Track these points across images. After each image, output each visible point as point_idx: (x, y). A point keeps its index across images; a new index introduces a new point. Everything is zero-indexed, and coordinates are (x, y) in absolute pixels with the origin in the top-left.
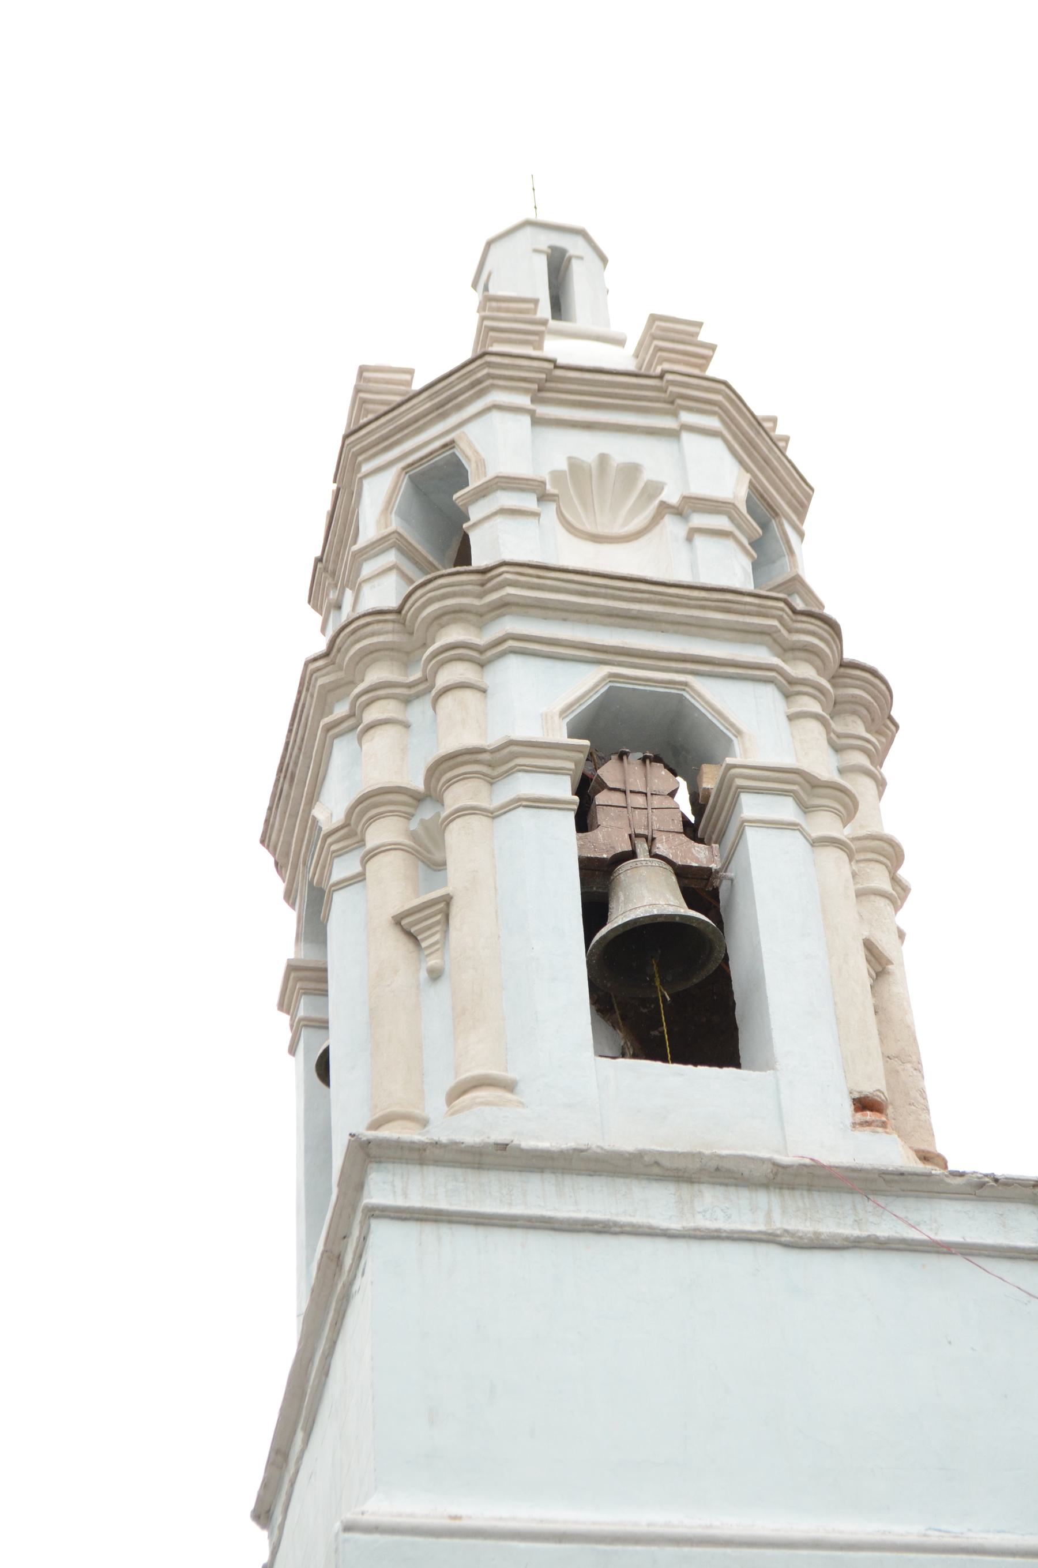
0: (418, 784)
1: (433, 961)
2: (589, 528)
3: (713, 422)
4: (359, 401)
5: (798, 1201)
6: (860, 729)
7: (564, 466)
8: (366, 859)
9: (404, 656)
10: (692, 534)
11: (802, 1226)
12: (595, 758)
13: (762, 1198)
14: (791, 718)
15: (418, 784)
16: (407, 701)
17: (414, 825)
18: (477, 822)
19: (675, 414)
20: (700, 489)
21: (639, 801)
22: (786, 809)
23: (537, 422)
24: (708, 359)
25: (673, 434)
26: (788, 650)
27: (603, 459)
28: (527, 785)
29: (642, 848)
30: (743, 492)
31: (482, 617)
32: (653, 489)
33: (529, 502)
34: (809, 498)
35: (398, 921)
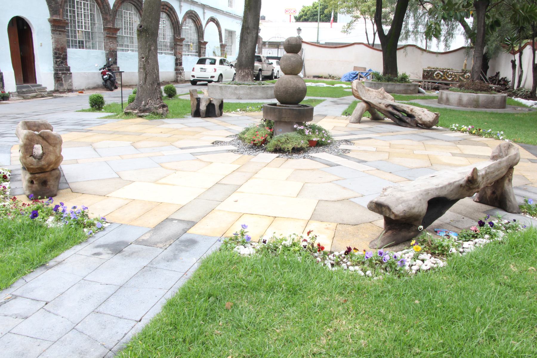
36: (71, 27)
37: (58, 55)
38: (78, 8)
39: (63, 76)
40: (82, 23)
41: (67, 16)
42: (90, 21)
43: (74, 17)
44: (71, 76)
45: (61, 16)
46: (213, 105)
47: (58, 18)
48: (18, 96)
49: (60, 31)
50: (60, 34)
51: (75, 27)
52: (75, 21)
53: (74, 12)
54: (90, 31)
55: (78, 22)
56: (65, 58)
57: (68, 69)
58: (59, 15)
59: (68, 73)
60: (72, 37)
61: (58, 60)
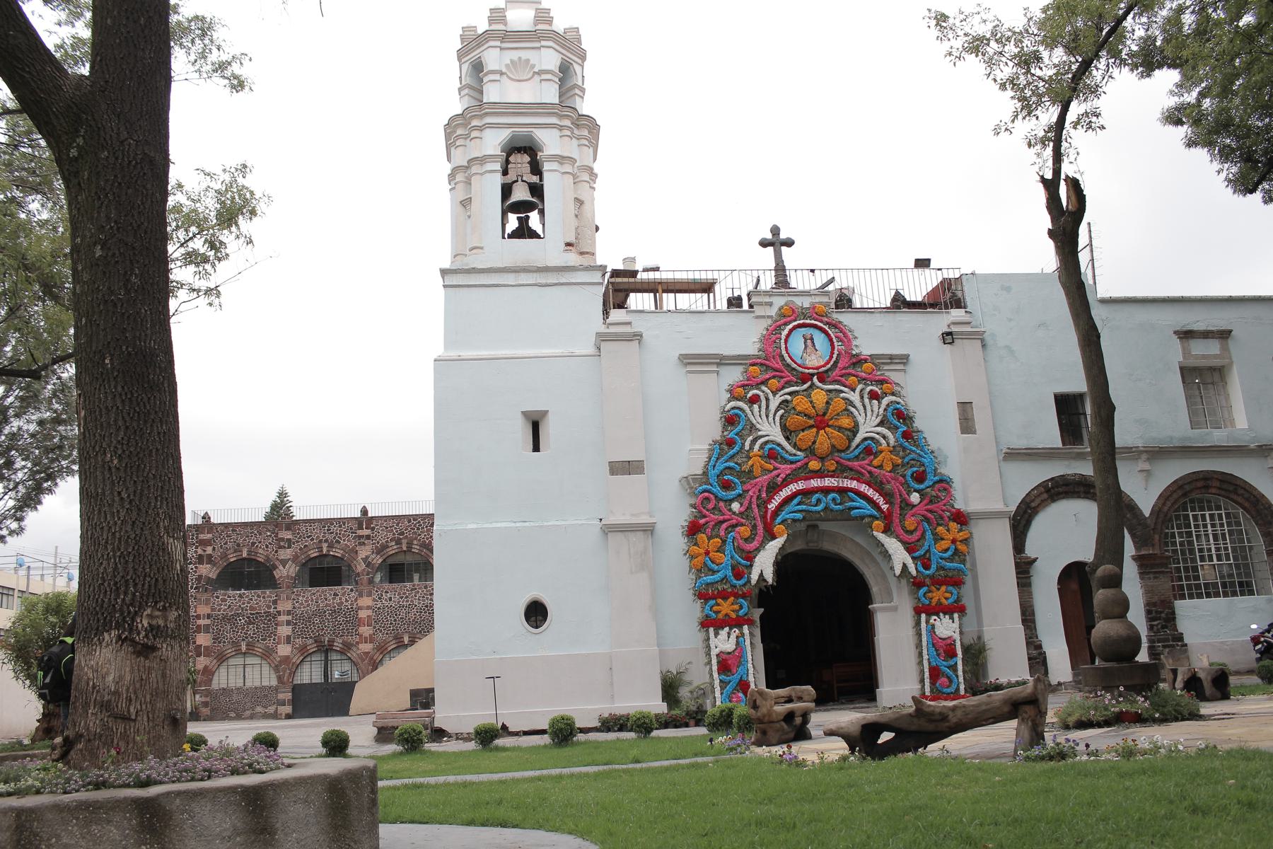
0: (466, 164)
1: (468, 214)
2: (517, 78)
3: (550, 43)
4: (462, 38)
5: (543, 275)
6: (586, 133)
7: (509, 62)
8: (455, 184)
9: (465, 125)
10: (541, 80)
11: (543, 281)
12: (508, 155)
13: (535, 274)
14: (561, 137)
15: (466, 164)
16: (466, 139)
17: (466, 175)
18: (478, 176)
19: (540, 41)
20: (544, 67)
21: (519, 165)
22: (555, 166)
23: (501, 49)
24: (552, 21)
25: (539, 48)
26: (561, 117)
27: (520, 58)
28: (489, 166)
29: (520, 180)
30: (558, 64)
31: (481, 117)
32: (533, 66)
33: (497, 77)
34: (585, 54)
35: (461, 202)
36: (1185, 561)
37: (1154, 614)
38: (1197, 526)
39: (1167, 650)
40: (1209, 550)
41: (1174, 544)
42: (1229, 545)
43: (1191, 543)
44: (1186, 651)
45: (1157, 546)
46: (1199, 679)
47: (1151, 552)
48: (1075, 688)
49: (1155, 573)
50: (1155, 578)
51: (1193, 560)
52: (1192, 551)
53: (1189, 534)
54: (1232, 561)
55: (1201, 550)
56: (1171, 618)
57: (1180, 638)
58: (1153, 545)
59: (1178, 645)
60: (1188, 578)
61: (1155, 623)
